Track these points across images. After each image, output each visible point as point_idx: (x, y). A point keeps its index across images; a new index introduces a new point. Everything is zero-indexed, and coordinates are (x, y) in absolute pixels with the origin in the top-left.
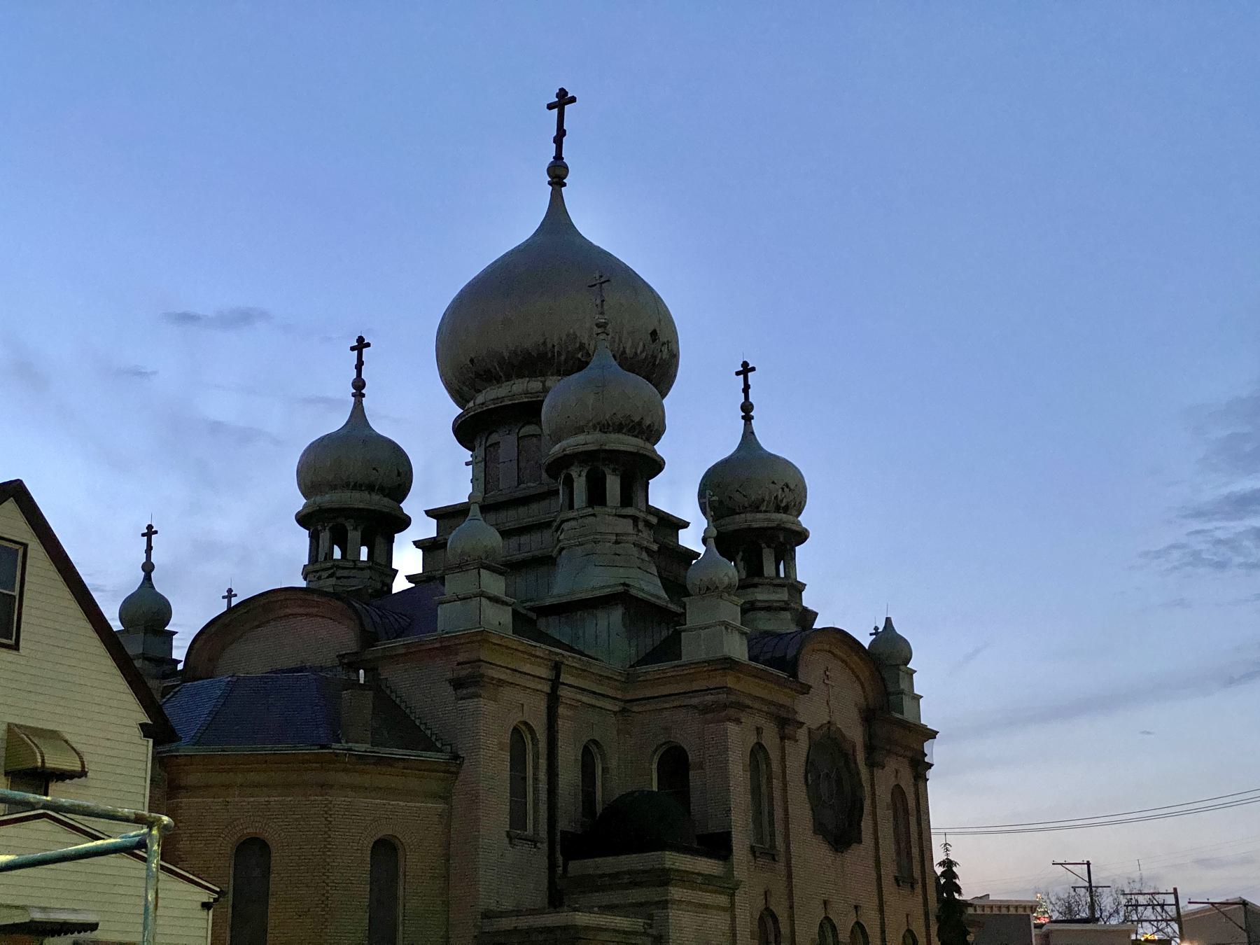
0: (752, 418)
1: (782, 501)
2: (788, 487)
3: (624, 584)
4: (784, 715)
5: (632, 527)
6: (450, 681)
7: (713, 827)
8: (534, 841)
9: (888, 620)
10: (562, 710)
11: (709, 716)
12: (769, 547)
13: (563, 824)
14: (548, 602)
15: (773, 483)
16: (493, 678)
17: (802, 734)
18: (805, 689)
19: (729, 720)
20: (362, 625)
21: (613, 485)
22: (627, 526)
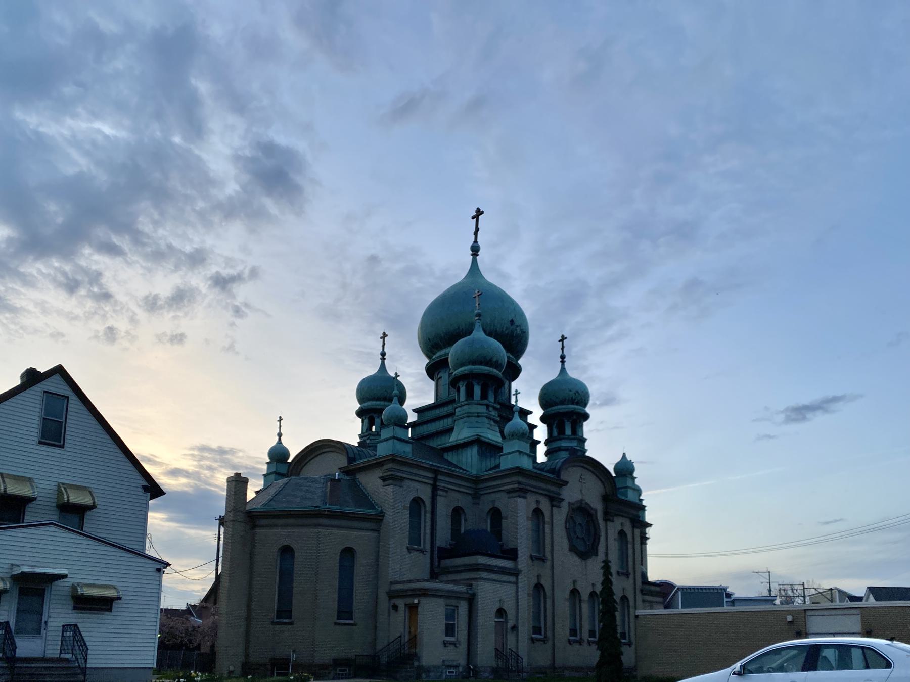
0: (565, 362)
1: (575, 399)
2: (577, 392)
3: (477, 435)
4: (551, 494)
5: (485, 410)
6: (380, 478)
7: (511, 545)
8: (422, 551)
9: (624, 454)
10: (440, 492)
11: (511, 495)
12: (568, 421)
13: (439, 543)
14: (448, 445)
15: (570, 391)
16: (397, 476)
17: (565, 505)
18: (566, 483)
19: (519, 496)
20: (347, 453)
21: (477, 390)
22: (482, 409)
